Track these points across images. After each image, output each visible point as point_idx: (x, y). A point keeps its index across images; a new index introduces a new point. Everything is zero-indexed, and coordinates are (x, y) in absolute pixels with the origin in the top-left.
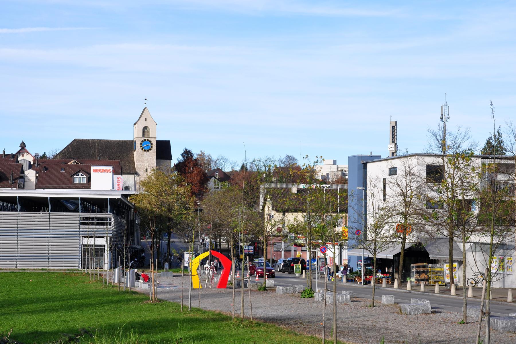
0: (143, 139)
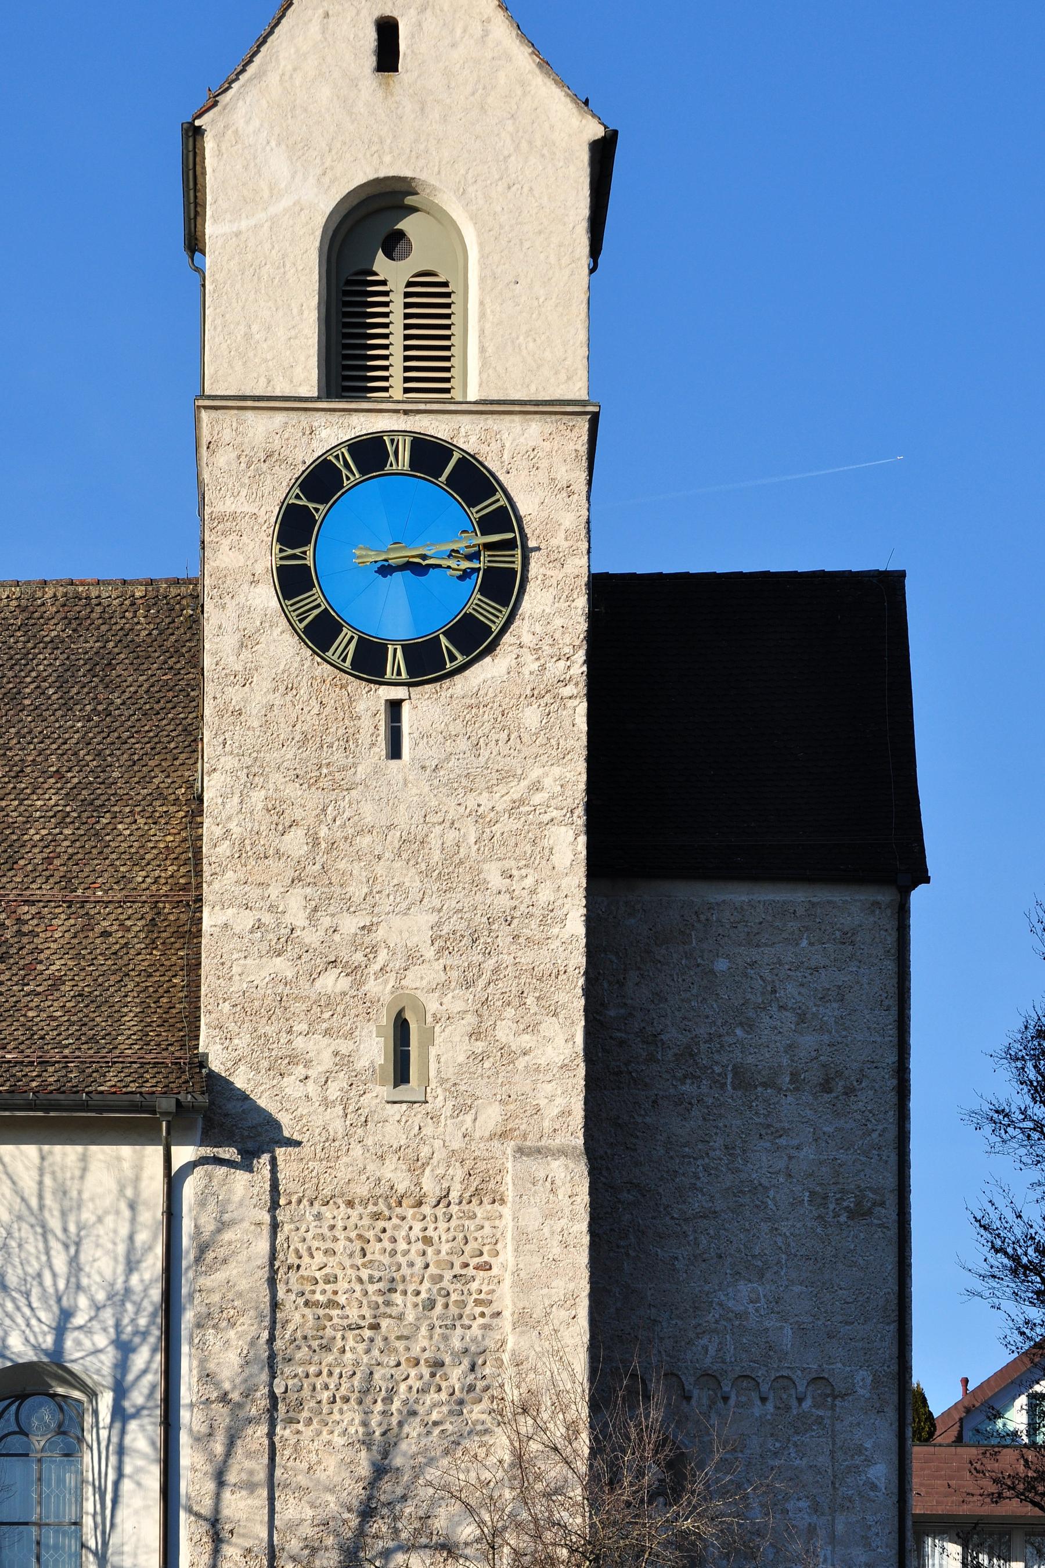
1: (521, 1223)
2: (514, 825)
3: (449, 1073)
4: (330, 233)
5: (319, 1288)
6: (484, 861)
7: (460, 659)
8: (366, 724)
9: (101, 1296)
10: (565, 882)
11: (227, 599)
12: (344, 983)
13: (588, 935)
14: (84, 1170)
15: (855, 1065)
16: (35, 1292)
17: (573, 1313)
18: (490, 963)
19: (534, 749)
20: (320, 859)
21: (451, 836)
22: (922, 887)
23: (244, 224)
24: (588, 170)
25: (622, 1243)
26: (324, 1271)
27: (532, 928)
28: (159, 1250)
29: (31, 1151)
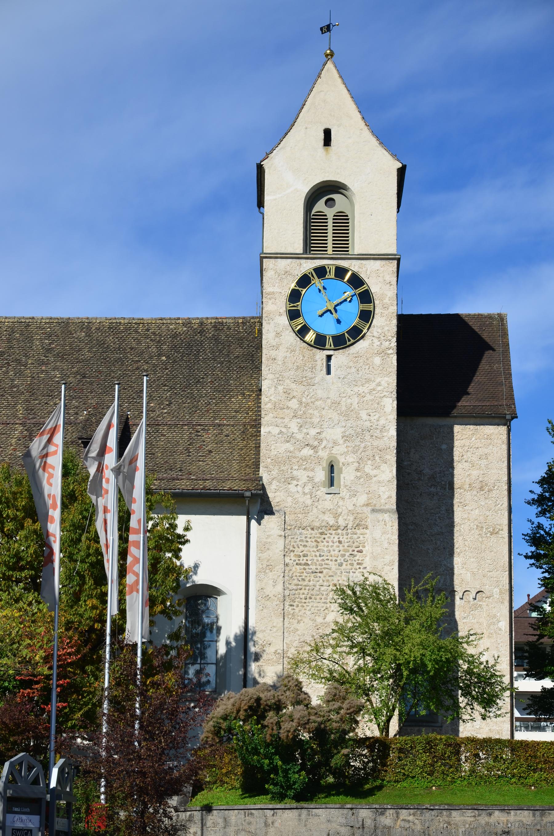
0: (308, 266)
1: (374, 536)
3: (348, 483)
4: (307, 199)
5: (301, 559)
6: (361, 410)
7: (352, 341)
8: (319, 363)
11: (271, 321)
12: (311, 452)
13: (398, 435)
17: (392, 567)
18: (363, 445)
21: (349, 401)
22: (515, 419)
24: (396, 178)
25: (409, 544)
26: (303, 553)
27: (377, 433)
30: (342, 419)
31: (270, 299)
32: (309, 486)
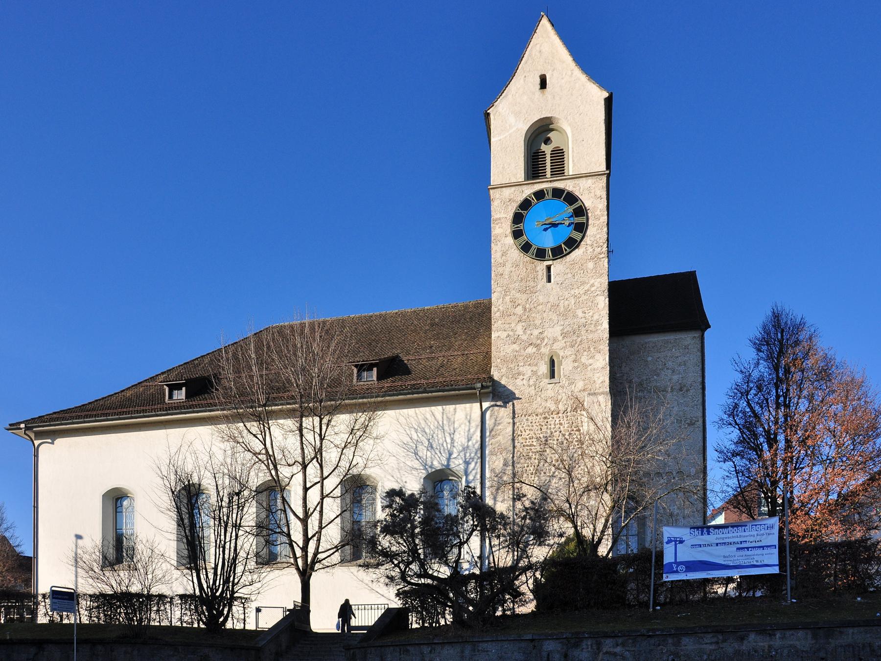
0: (529, 191)
2: (586, 297)
3: (567, 373)
5: (527, 441)
8: (540, 273)
9: (461, 448)
10: (602, 313)
11: (498, 242)
12: (534, 350)
14: (455, 412)
15: (690, 383)
16: (442, 448)
18: (579, 339)
19: (592, 274)
20: (527, 314)
21: (567, 303)
23: (502, 137)
27: (592, 328)
28: (478, 434)
29: (440, 408)
30: (561, 318)
31: (497, 224)
32: (534, 378)
